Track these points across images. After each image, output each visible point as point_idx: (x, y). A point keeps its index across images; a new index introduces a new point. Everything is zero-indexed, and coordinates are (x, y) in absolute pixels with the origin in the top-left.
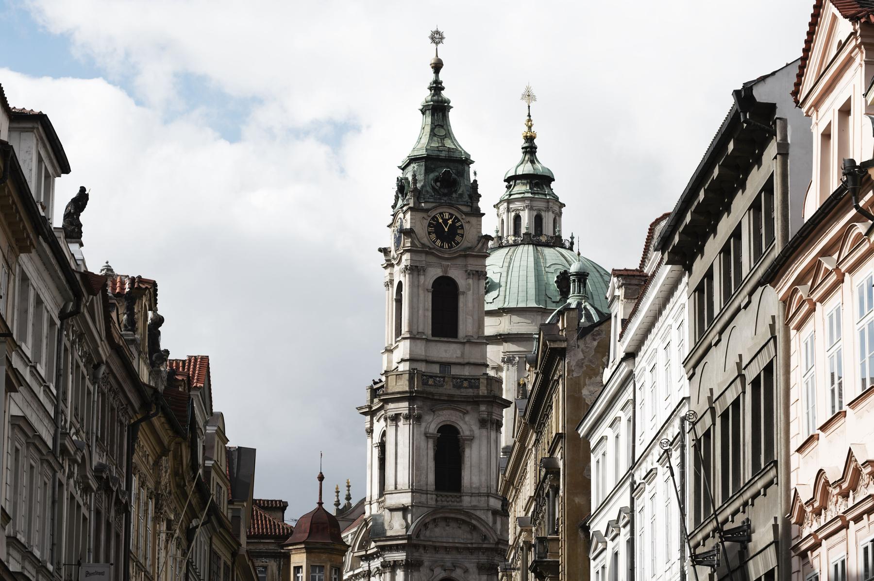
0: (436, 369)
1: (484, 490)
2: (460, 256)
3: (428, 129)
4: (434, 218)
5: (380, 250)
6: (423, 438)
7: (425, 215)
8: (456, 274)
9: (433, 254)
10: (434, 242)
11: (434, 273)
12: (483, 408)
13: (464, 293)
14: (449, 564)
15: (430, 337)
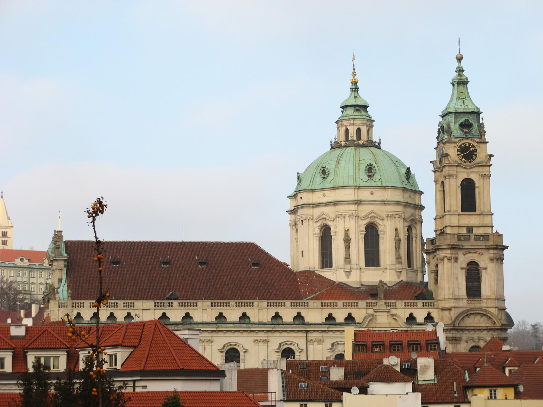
0: (464, 231)
1: (493, 297)
2: (476, 166)
3: (455, 95)
4: (460, 147)
5: (431, 162)
6: (459, 269)
7: (455, 145)
8: (474, 177)
9: (460, 166)
10: (461, 160)
11: (463, 176)
12: (492, 251)
13: (479, 187)
14: (476, 338)
15: (461, 213)
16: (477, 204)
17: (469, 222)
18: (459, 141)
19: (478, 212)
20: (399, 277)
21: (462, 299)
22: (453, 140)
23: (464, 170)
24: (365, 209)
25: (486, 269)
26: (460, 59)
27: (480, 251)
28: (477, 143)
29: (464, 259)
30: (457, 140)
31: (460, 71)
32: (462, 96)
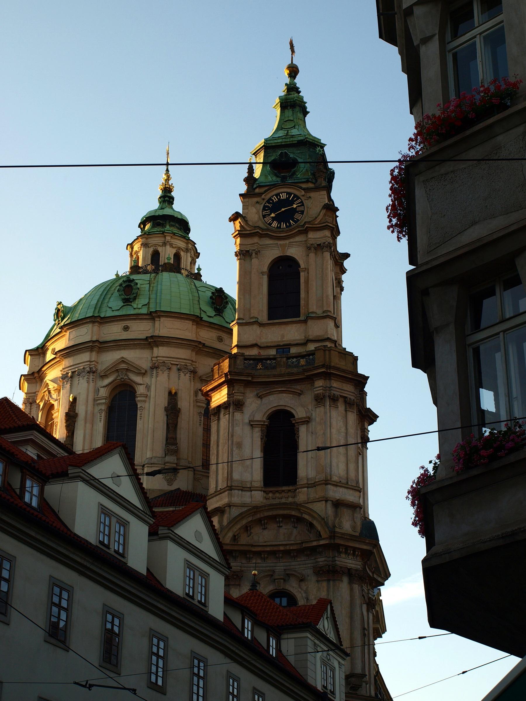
2: (300, 233)
4: (268, 202)
8: (295, 251)
10: (270, 224)
12: (319, 383)
16: (302, 302)
17: (283, 336)
18: (265, 191)
19: (302, 318)
20: (170, 482)
21: (250, 489)
22: (257, 191)
23: (276, 242)
24: (110, 358)
25: (307, 421)
26: (293, 71)
27: (298, 387)
28: (304, 189)
29: (257, 407)
30: (262, 190)
31: (292, 88)
32: (289, 125)
